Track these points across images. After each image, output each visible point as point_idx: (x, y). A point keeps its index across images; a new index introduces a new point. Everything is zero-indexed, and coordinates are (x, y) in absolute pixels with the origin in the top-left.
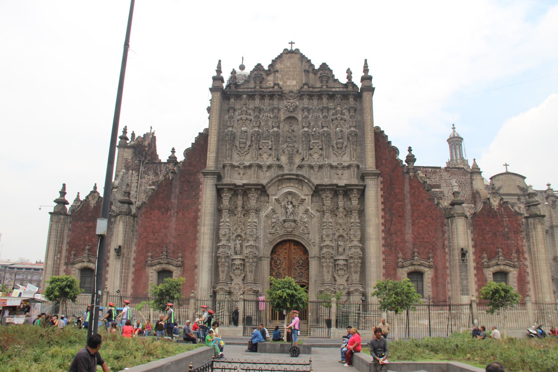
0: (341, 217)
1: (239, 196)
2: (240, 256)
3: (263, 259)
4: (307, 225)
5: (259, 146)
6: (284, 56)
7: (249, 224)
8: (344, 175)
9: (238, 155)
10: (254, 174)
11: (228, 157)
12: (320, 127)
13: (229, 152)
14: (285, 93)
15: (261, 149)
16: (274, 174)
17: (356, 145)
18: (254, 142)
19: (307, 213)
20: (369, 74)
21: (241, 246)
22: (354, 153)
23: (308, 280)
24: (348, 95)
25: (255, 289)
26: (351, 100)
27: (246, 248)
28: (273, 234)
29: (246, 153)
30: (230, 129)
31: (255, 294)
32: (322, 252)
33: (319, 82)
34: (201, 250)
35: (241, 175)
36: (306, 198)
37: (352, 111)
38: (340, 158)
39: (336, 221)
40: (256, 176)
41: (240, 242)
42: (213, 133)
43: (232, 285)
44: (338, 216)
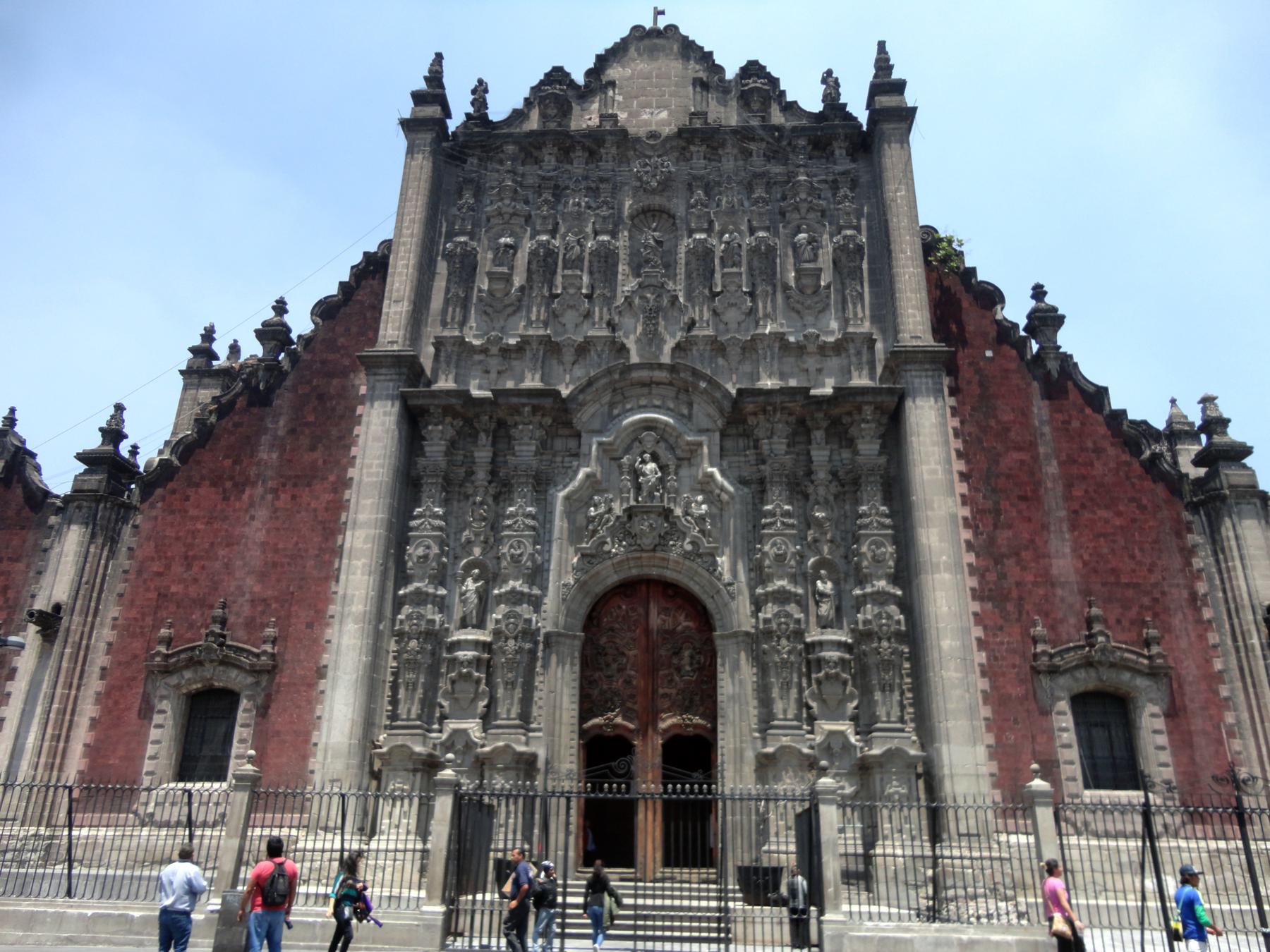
0: (821, 500)
20: (896, 75)
29: (510, 310)
42: (404, 244)
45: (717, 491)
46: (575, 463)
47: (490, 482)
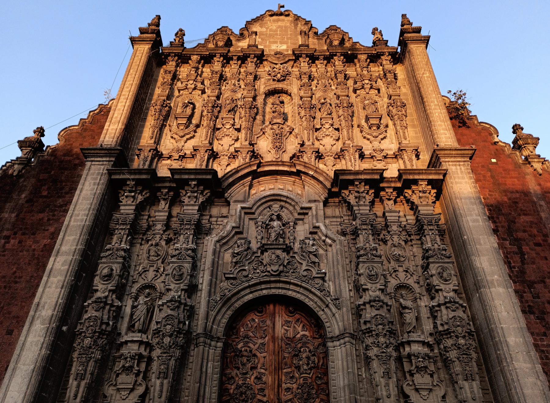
36: (312, 205)
44: (389, 243)
45: (324, 238)
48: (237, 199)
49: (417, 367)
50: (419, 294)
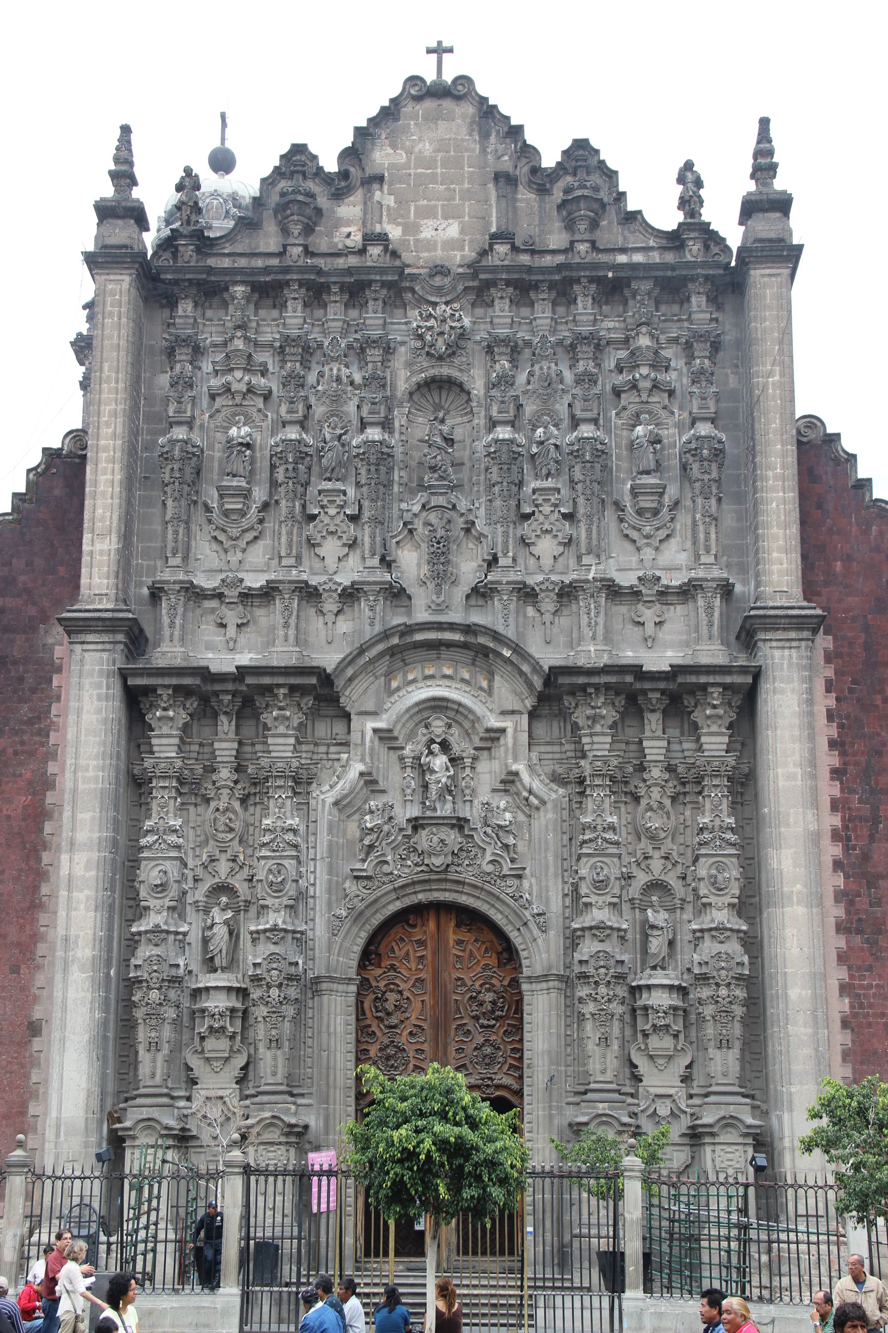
0: (655, 806)
1: (223, 718)
2: (225, 976)
3: (324, 986)
4: (511, 841)
5: (304, 506)
6: (408, 108)
7: (266, 839)
8: (666, 626)
9: (215, 546)
10: (286, 625)
11: (174, 555)
12: (566, 424)
13: (176, 532)
14: (414, 277)
15: (313, 518)
16: (372, 624)
17: (719, 500)
18: (282, 489)
19: (513, 789)
20: (779, 184)
21: (231, 933)
22: (707, 534)
23: (521, 1077)
24: (685, 280)
25: (293, 1121)
26: (698, 301)
27: (254, 940)
28: (368, 878)
29: (249, 536)
30: (180, 433)
31: (293, 1139)
32: (577, 956)
33: (558, 224)
34: (60, 953)
35: (231, 631)
36: (508, 723)
37: (701, 349)
38: (648, 553)
39: (633, 823)
40: (292, 632)
41: (229, 914)
42: (106, 449)
43: (195, 1105)
44: (644, 802)
45: (525, 794)
46: (344, 756)
47: (236, 782)
48: (363, 709)
49: (654, 1026)
50: (682, 899)
